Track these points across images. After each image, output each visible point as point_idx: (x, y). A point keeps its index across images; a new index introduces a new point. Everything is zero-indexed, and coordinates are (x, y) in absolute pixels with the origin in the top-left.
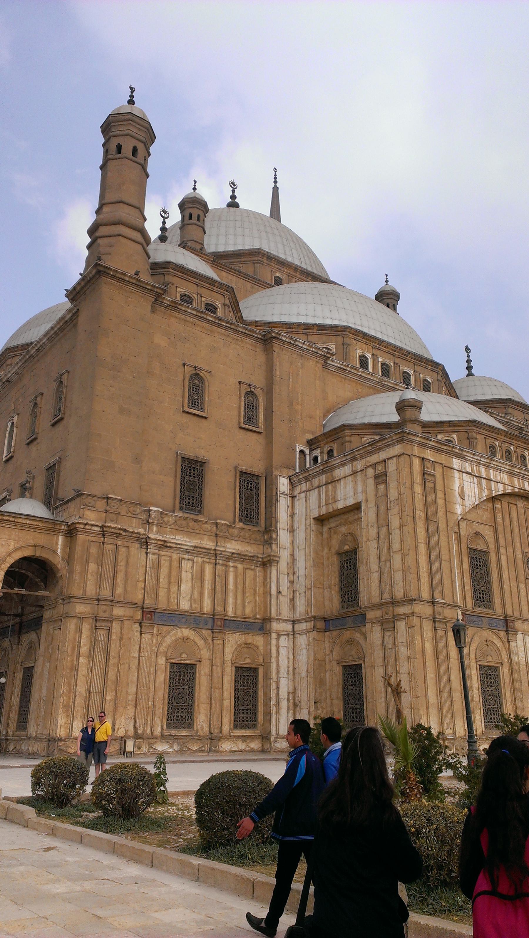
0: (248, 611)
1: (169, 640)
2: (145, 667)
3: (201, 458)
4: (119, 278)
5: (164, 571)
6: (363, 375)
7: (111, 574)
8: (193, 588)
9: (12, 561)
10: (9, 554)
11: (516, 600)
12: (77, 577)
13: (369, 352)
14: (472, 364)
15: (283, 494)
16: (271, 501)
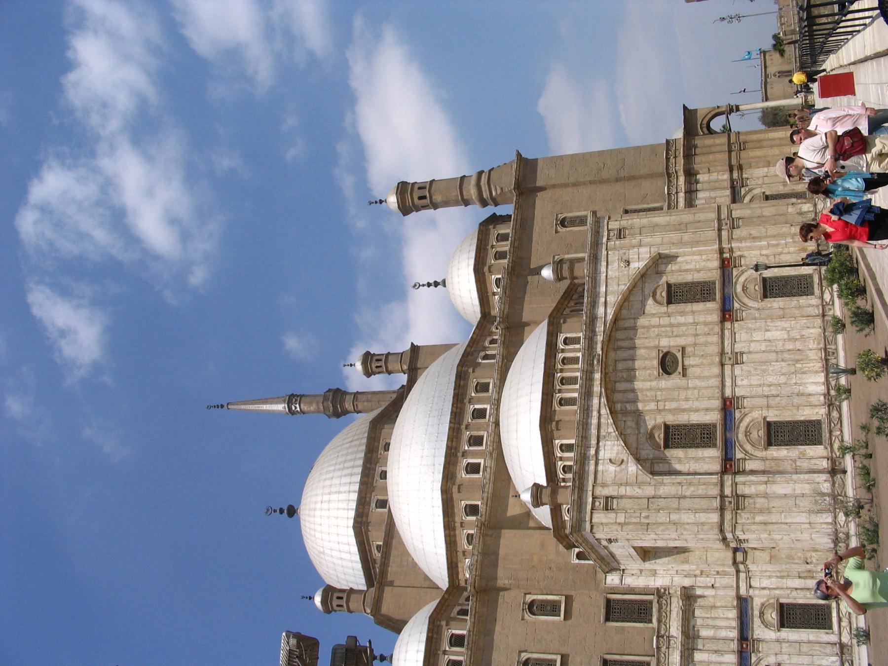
6: (488, 477)
14: (432, 281)
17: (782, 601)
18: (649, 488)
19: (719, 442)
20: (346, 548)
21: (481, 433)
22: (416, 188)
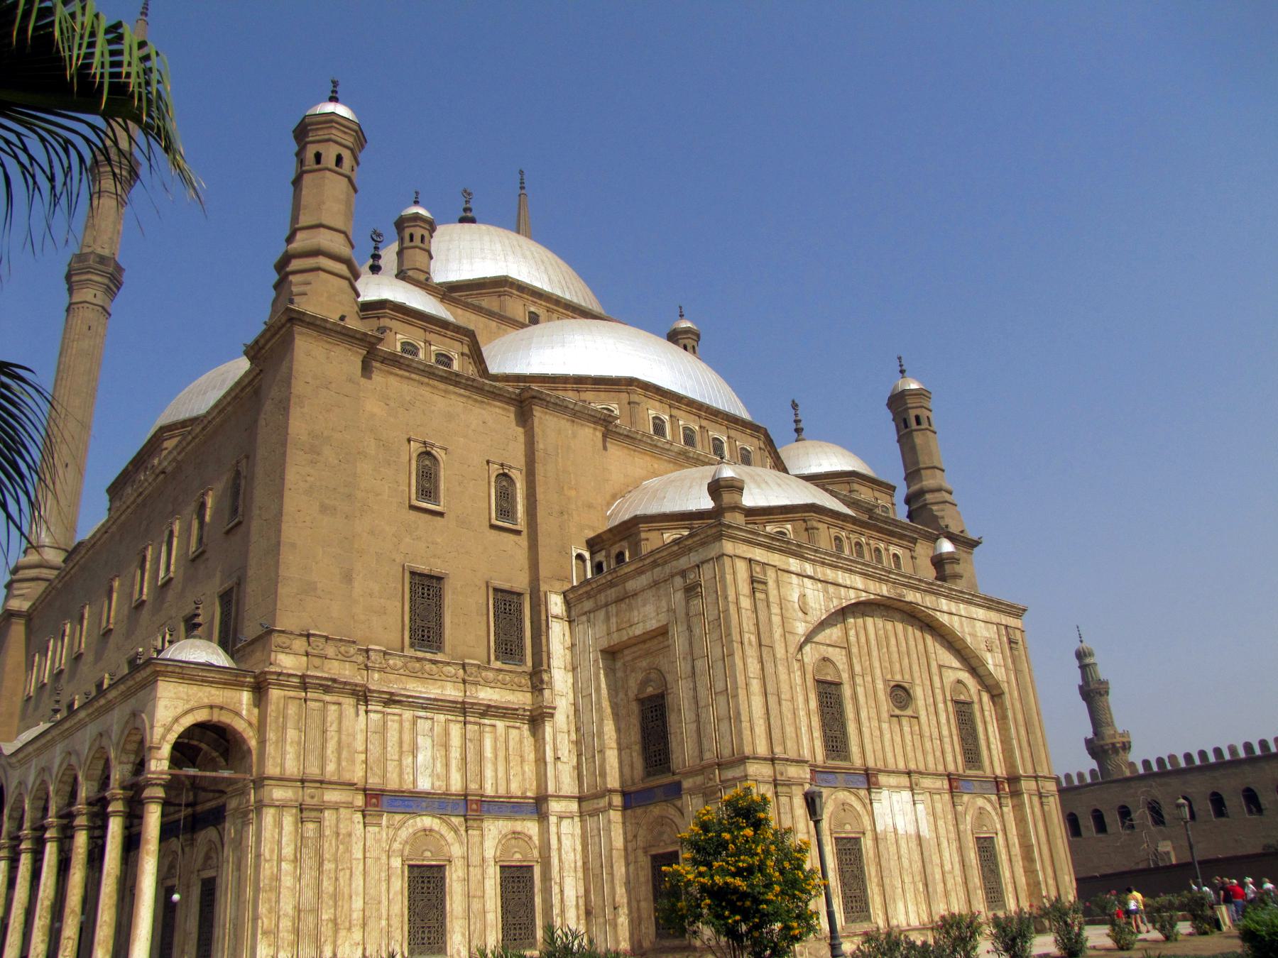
2: (373, 872)
3: (437, 571)
4: (319, 326)
7: (318, 744)
9: (181, 729)
10: (176, 720)
11: (878, 747)
12: (270, 749)
13: (664, 412)
14: (801, 425)
15: (556, 617)
16: (539, 628)
18: (783, 651)
19: (831, 763)
21: (699, 446)
22: (928, 413)
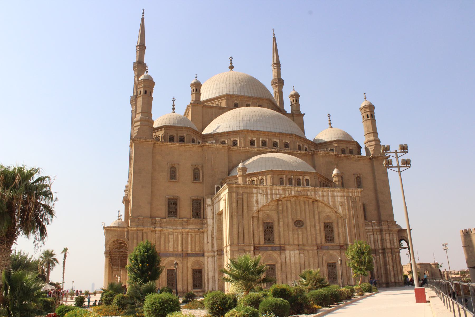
0: (197, 249)
1: (166, 262)
3: (175, 197)
5: (162, 239)
8: (174, 244)
10: (110, 239)
12: (130, 245)
15: (209, 205)
17: (203, 270)
20: (217, 92)
21: (267, 145)
